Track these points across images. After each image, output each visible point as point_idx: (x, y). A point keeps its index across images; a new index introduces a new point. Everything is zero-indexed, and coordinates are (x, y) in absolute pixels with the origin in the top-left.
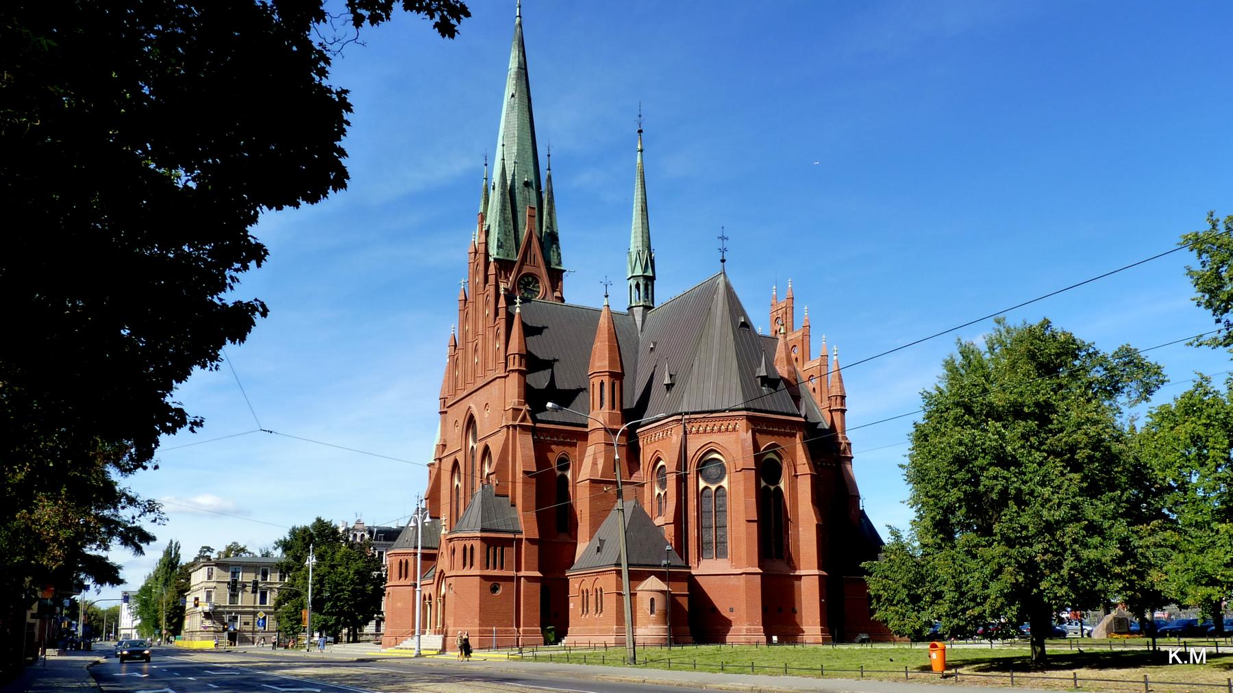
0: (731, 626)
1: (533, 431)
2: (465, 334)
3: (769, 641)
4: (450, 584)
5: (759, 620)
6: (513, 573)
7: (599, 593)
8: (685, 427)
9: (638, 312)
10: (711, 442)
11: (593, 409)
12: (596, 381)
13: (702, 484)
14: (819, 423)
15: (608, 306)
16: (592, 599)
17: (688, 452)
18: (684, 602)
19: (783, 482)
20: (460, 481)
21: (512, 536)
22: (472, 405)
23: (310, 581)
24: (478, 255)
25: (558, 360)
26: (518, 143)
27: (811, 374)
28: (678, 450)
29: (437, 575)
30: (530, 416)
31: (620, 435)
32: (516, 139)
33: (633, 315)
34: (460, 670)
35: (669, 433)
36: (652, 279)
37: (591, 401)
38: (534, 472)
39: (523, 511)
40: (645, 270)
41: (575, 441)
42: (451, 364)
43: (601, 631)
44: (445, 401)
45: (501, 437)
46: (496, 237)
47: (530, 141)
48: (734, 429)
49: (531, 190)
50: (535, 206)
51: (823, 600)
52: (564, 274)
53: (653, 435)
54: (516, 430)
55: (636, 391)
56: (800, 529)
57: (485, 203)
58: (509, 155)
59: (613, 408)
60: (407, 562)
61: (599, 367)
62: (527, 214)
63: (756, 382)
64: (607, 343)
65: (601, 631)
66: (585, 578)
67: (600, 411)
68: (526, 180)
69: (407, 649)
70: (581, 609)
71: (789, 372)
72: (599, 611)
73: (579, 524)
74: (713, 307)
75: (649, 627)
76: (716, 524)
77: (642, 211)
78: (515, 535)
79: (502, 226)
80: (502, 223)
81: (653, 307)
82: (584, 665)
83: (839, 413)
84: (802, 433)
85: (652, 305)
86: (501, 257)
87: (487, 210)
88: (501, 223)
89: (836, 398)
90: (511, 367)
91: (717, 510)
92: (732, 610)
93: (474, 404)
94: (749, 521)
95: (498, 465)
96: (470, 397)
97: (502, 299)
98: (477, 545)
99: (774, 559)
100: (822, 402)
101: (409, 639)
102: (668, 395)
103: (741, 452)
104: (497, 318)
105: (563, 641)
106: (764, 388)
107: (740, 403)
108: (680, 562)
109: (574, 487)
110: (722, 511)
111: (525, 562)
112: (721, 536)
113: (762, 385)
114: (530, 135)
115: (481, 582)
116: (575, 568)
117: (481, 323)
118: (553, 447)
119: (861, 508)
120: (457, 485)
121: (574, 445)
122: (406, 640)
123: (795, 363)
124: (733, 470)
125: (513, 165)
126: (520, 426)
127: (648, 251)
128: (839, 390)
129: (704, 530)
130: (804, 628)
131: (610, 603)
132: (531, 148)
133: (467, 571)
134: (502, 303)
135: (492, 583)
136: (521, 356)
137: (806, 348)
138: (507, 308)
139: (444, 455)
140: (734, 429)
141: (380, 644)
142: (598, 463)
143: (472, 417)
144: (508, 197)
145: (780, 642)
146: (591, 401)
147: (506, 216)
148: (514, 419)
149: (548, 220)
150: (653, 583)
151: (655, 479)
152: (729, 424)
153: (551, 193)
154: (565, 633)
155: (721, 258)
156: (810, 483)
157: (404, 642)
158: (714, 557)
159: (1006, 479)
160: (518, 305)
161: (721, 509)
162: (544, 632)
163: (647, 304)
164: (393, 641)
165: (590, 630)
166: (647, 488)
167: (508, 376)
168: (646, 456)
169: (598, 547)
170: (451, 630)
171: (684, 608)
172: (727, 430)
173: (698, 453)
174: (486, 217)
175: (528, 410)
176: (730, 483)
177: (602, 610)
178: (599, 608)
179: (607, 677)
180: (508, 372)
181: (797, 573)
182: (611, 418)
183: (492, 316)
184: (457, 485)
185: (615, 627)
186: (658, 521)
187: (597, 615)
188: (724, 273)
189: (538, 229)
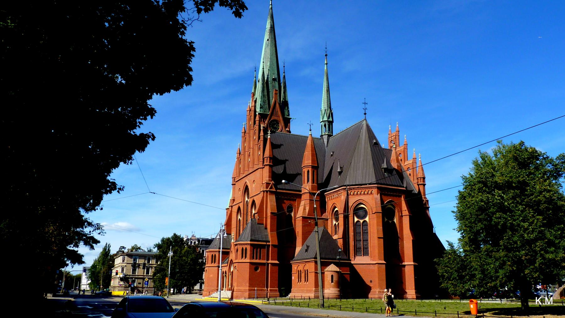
2: (244, 148)
4: (235, 266)
6: (265, 261)
7: (306, 272)
8: (348, 192)
9: (325, 138)
12: (305, 170)
13: (356, 219)
15: (311, 135)
16: (303, 275)
17: (349, 204)
18: (348, 277)
21: (265, 243)
22: (247, 181)
23: (170, 264)
24: (251, 111)
25: (288, 160)
27: (408, 167)
28: (344, 203)
30: (274, 186)
32: (269, 59)
33: (323, 139)
35: (340, 195)
36: (332, 122)
37: (303, 180)
38: (276, 213)
39: (270, 231)
41: (295, 198)
43: (307, 290)
44: (234, 179)
45: (261, 196)
47: (276, 60)
48: (371, 193)
49: (276, 82)
50: (278, 89)
51: (416, 277)
52: (291, 120)
55: (324, 175)
56: (404, 242)
57: (255, 88)
59: (313, 183)
61: (307, 163)
62: (274, 93)
63: (382, 171)
64: (311, 152)
66: (300, 265)
67: (307, 184)
68: (274, 77)
69: (214, 297)
70: (297, 280)
72: (306, 281)
73: (297, 238)
74: (361, 135)
75: (331, 289)
77: (327, 91)
78: (266, 243)
81: (332, 135)
82: (299, 308)
83: (422, 186)
85: (332, 134)
86: (262, 113)
87: (255, 91)
88: (262, 97)
89: (421, 179)
91: (364, 232)
92: (371, 282)
93: (248, 181)
94: (379, 238)
96: (246, 177)
97: (262, 132)
98: (248, 247)
100: (414, 180)
101: (215, 293)
102: (339, 177)
104: (259, 140)
105: (289, 295)
106: (385, 174)
107: (374, 180)
109: (295, 220)
110: (366, 233)
111: (271, 256)
113: (385, 172)
114: (275, 57)
117: (252, 142)
118: (285, 201)
119: (434, 232)
120: (240, 219)
121: (295, 200)
122: (214, 293)
123: (400, 162)
124: (371, 213)
125: (268, 71)
126: (269, 191)
128: (422, 175)
130: (407, 291)
131: (312, 277)
132: (276, 63)
133: (243, 260)
134: (262, 133)
136: (270, 158)
137: (406, 155)
138: (264, 136)
139: (234, 204)
140: (371, 193)
141: (202, 294)
143: (247, 186)
144: (265, 85)
146: (303, 180)
147: (264, 94)
148: (267, 188)
149: (284, 96)
150: (332, 268)
151: (333, 217)
152: (369, 191)
153: (285, 83)
154: (290, 291)
155: (364, 113)
156: (408, 219)
158: (362, 255)
161: (365, 231)
162: (280, 291)
163: (330, 134)
164: (208, 294)
167: (264, 167)
168: (329, 205)
169: (306, 249)
170: (235, 288)
171: (348, 280)
172: (368, 194)
173: (354, 204)
174: (255, 94)
175: (273, 184)
176: (369, 219)
178: (306, 279)
180: (264, 165)
181: (403, 264)
182: (313, 188)
183: (257, 139)
184: (240, 219)
185: (314, 289)
186: (335, 237)
187: (305, 283)
188: (366, 119)
189: (279, 100)
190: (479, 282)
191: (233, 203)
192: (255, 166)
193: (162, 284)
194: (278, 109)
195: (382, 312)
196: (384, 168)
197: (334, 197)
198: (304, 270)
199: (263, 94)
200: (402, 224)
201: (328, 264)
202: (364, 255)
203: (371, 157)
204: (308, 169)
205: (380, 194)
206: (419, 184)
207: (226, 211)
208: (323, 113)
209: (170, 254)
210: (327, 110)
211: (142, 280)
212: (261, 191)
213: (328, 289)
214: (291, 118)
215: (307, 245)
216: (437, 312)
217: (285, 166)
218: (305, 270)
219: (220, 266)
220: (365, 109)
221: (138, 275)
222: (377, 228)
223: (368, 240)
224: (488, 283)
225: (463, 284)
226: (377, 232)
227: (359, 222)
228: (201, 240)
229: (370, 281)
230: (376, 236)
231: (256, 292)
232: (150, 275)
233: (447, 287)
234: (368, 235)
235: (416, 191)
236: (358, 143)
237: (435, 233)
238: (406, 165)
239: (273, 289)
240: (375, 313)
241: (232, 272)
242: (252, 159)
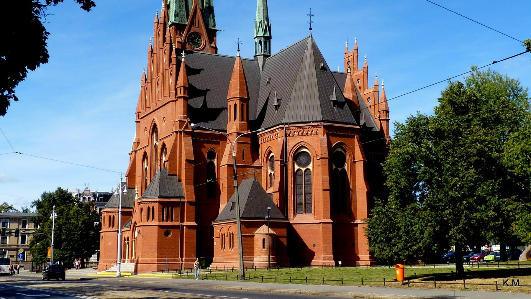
0: (315, 255)
1: (192, 134)
2: (152, 73)
3: (337, 265)
4: (139, 231)
5: (331, 251)
7: (231, 235)
8: (286, 132)
9: (260, 59)
10: (302, 142)
11: (230, 121)
12: (232, 104)
13: (297, 167)
14: (374, 127)
15: (239, 57)
16: (227, 239)
17: (288, 148)
18: (284, 241)
19: (346, 165)
20: (147, 165)
21: (179, 200)
22: (155, 118)
23: (53, 229)
24: (159, 24)
25: (209, 90)
31: (240, 137)
33: (257, 61)
34: (140, 284)
35: (276, 136)
36: (270, 38)
37: (229, 116)
40: (265, 32)
41: (219, 141)
43: (232, 259)
44: (139, 115)
46: (174, 9)
48: (316, 134)
52: (217, 32)
53: (267, 137)
61: (234, 95)
63: (330, 104)
64: (239, 80)
65: (232, 259)
66: (223, 226)
67: (234, 122)
69: (113, 272)
70: (221, 246)
71: (353, 97)
72: (231, 247)
73: (221, 192)
74: (304, 57)
78: (180, 200)
81: (270, 56)
82: (215, 281)
83: (385, 121)
84: (358, 135)
85: (269, 54)
86: (177, 22)
89: (383, 112)
90: (179, 95)
91: (306, 183)
92: (314, 245)
93: (156, 117)
94: (324, 190)
97: (174, 52)
98: (156, 206)
100: (375, 114)
101: (115, 266)
102: (276, 112)
103: (320, 147)
105: (211, 266)
106: (335, 108)
108: (281, 216)
110: (309, 184)
111: (187, 217)
112: (308, 200)
113: (334, 106)
115: (158, 230)
117: (161, 67)
118: (205, 144)
120: (146, 168)
122: (113, 266)
123: (359, 90)
126: (183, 131)
127: (267, 21)
128: (385, 107)
129: (298, 196)
130: (360, 256)
131: (237, 242)
133: (150, 223)
134: (174, 55)
135: (165, 230)
136: (185, 88)
138: (177, 58)
139: (139, 148)
140: (316, 134)
141: (97, 269)
145: (343, 266)
146: (229, 116)
148: (180, 127)
150: (264, 229)
152: (313, 130)
155: (310, 27)
156: (363, 166)
157: (112, 267)
158: (304, 213)
159: (432, 174)
161: (308, 183)
163: (266, 54)
164: (105, 267)
165: (226, 259)
166: (263, 170)
167: (177, 100)
168: (263, 149)
169: (231, 207)
170: (140, 259)
172: (311, 134)
173: (294, 148)
176: (313, 166)
178: (231, 245)
179: (223, 287)
180: (177, 98)
181: (356, 222)
182: (241, 127)
183: (168, 62)
184: (146, 168)
188: (311, 36)
189: (201, 4)
190: (404, 244)
191: (137, 147)
192: (165, 98)
193: (43, 256)
194: (200, 18)
195: (307, 282)
196: (333, 101)
200: (355, 172)
201: (258, 225)
202: (305, 213)
203: (317, 86)
205: (327, 135)
206: (382, 119)
207: (129, 156)
209: (53, 215)
210: (262, 22)
211: (16, 251)
212: (173, 131)
213: (258, 256)
214: (218, 30)
216: (385, 280)
217: (205, 98)
218: (230, 233)
219: (119, 231)
220: (311, 23)
221: (9, 245)
222: (322, 177)
224: (413, 245)
225: (391, 247)
227: (300, 171)
228: (98, 194)
230: (321, 189)
231: (166, 263)
232: (26, 244)
233: (374, 251)
234: (311, 187)
235: (378, 128)
236: (301, 68)
238: (365, 93)
239: (191, 259)
240: (300, 284)
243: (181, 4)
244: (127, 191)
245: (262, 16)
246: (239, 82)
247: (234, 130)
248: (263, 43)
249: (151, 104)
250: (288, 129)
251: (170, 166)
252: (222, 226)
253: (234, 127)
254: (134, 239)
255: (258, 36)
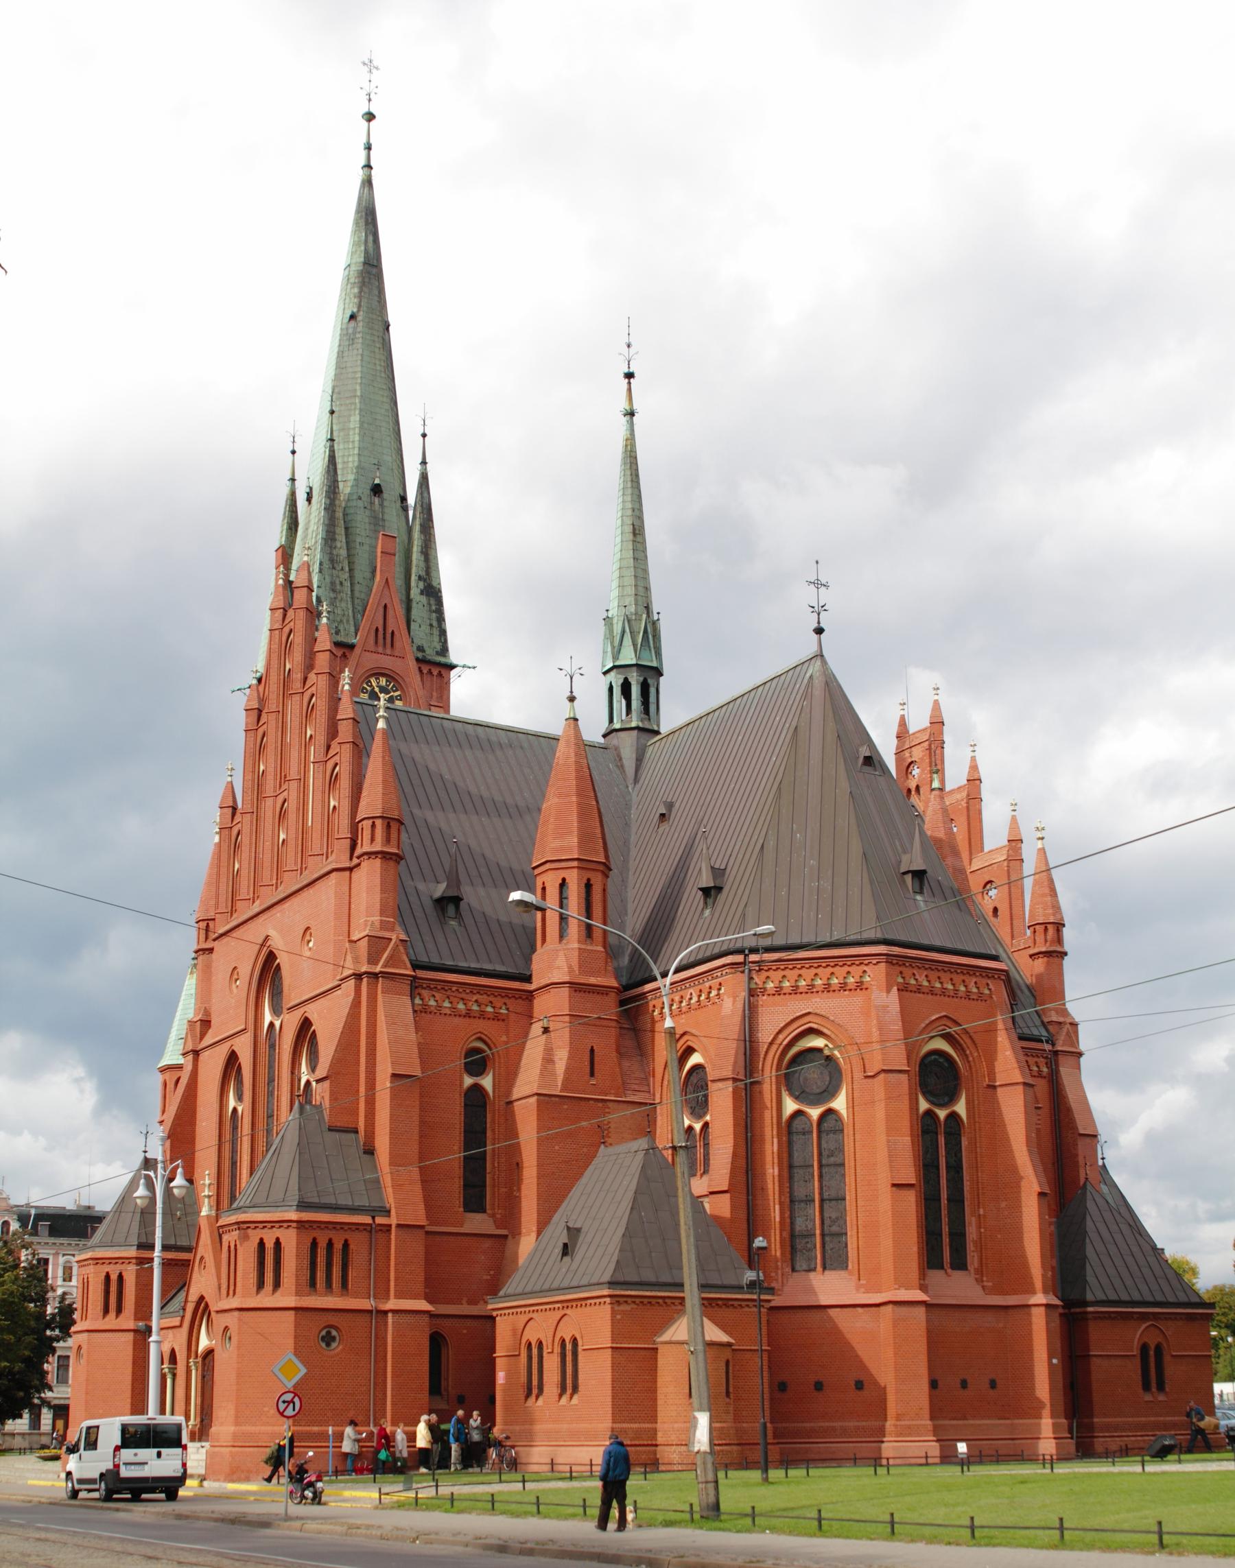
2: (256, 784)
4: (226, 1329)
9: (627, 744)
10: (809, 1013)
13: (790, 1106)
16: (552, 1364)
20: (240, 1098)
22: (272, 933)
26: (361, 410)
29: (190, 1308)
35: (714, 993)
36: (658, 672)
39: (391, 1164)
42: (225, 846)
44: (208, 925)
45: (344, 998)
51: (1055, 1361)
52: (453, 673)
54: (378, 982)
58: (342, 434)
60: (121, 1277)
62: (379, 550)
64: (574, 799)
66: (534, 1315)
72: (569, 1391)
76: (821, 1194)
78: (373, 1218)
79: (326, 571)
80: (326, 565)
89: (1046, 929)
91: (824, 1162)
95: (337, 1062)
98: (290, 1239)
99: (949, 1271)
102: (707, 912)
104: (334, 744)
106: (919, 897)
111: (396, 1279)
112: (834, 1221)
116: (510, 1291)
119: (1100, 1163)
120: (235, 1110)
124: (858, 1075)
126: (381, 972)
133: (267, 1299)
140: (860, 986)
142: (556, 1059)
143: (271, 956)
145: (977, 1458)
147: (335, 552)
148: (373, 960)
155: (816, 625)
156: (1021, 1103)
158: (819, 1268)
160: (382, 713)
161: (832, 1160)
163: (647, 726)
167: (359, 865)
169: (565, 1245)
172: (843, 987)
173: (781, 1037)
174: (292, 556)
177: (575, 1389)
180: (358, 857)
183: (321, 739)
184: (235, 1110)
191: (201, 1039)
192: (311, 862)
197: (684, 1004)
198: (557, 1339)
199: (331, 553)
202: (824, 1268)
204: (563, 874)
208: (617, 629)
215: (571, 1225)
218: (563, 1341)
222: (888, 1141)
223: (844, 1199)
226: (890, 1161)
228: (33, 1212)
229: (853, 1383)
231: (331, 1444)
234: (844, 1175)
237: (1104, 1165)
241: (210, 1353)
242: (297, 829)
243: (338, 577)
244: (184, 1183)
245: (632, 599)
246: (574, 808)
247: (560, 974)
248: (635, 691)
249: (279, 870)
250: (760, 970)
251: (334, 1097)
252: (531, 1315)
253: (561, 961)
254: (197, 1357)
255: (617, 664)
